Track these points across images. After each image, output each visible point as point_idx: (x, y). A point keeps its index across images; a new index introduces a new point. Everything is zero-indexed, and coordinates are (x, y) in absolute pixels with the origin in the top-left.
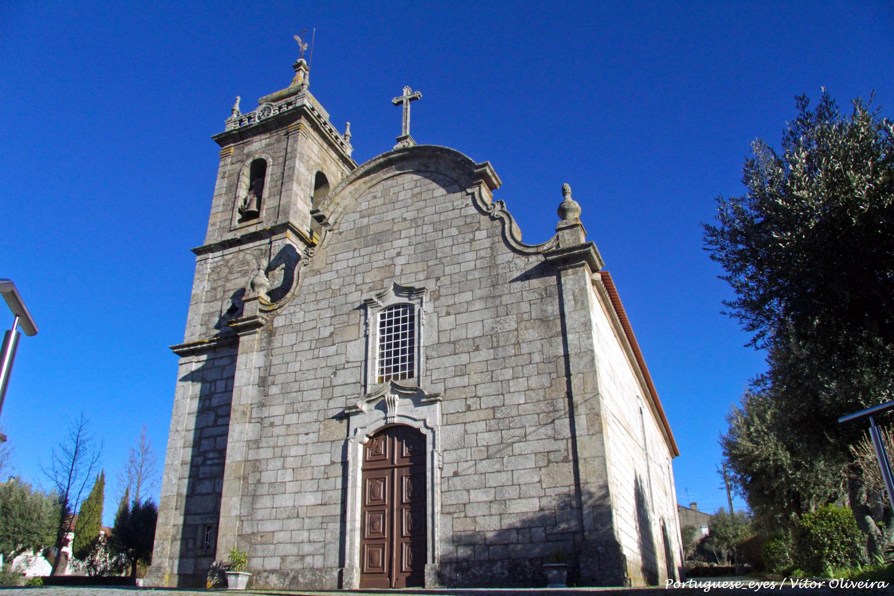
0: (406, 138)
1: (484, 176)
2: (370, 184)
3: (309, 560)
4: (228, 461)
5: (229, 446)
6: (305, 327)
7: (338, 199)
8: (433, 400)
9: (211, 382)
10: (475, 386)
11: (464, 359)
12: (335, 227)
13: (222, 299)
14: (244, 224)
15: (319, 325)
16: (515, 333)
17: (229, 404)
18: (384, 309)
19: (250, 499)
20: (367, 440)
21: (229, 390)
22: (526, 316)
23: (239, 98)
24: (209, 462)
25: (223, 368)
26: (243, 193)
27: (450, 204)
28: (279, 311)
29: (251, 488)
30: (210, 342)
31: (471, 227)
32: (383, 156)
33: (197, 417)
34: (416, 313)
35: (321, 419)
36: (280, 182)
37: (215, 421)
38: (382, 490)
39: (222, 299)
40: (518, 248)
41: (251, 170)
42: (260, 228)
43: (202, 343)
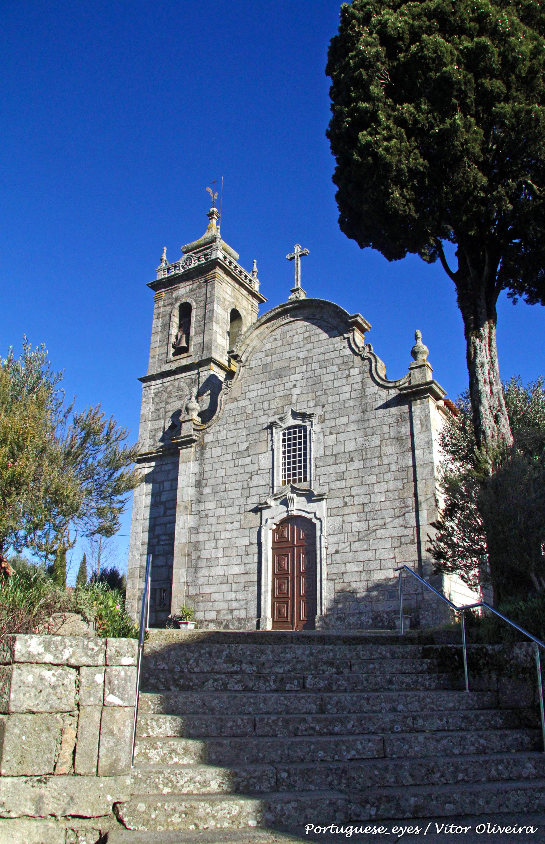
0: (298, 289)
1: (357, 324)
2: (271, 329)
3: (236, 613)
4: (176, 543)
5: (176, 532)
6: (228, 442)
7: (248, 341)
8: (320, 498)
9: (159, 483)
10: (350, 488)
11: (343, 467)
12: (247, 364)
13: (165, 418)
14: (177, 357)
15: (238, 441)
16: (379, 448)
17: (175, 499)
18: (285, 429)
19: (193, 570)
20: (274, 527)
21: (174, 489)
22: (386, 436)
23: (165, 248)
24: (162, 543)
25: (168, 472)
26: (174, 331)
27: (331, 346)
28: (208, 430)
29: (194, 562)
30: (157, 452)
31: (347, 365)
32: (281, 307)
33: (151, 509)
34: (308, 433)
35: (242, 511)
36: (202, 323)
37: (165, 512)
38: (286, 563)
39: (165, 418)
40: (382, 383)
41: (180, 311)
42: (190, 361)
43: (152, 453)
